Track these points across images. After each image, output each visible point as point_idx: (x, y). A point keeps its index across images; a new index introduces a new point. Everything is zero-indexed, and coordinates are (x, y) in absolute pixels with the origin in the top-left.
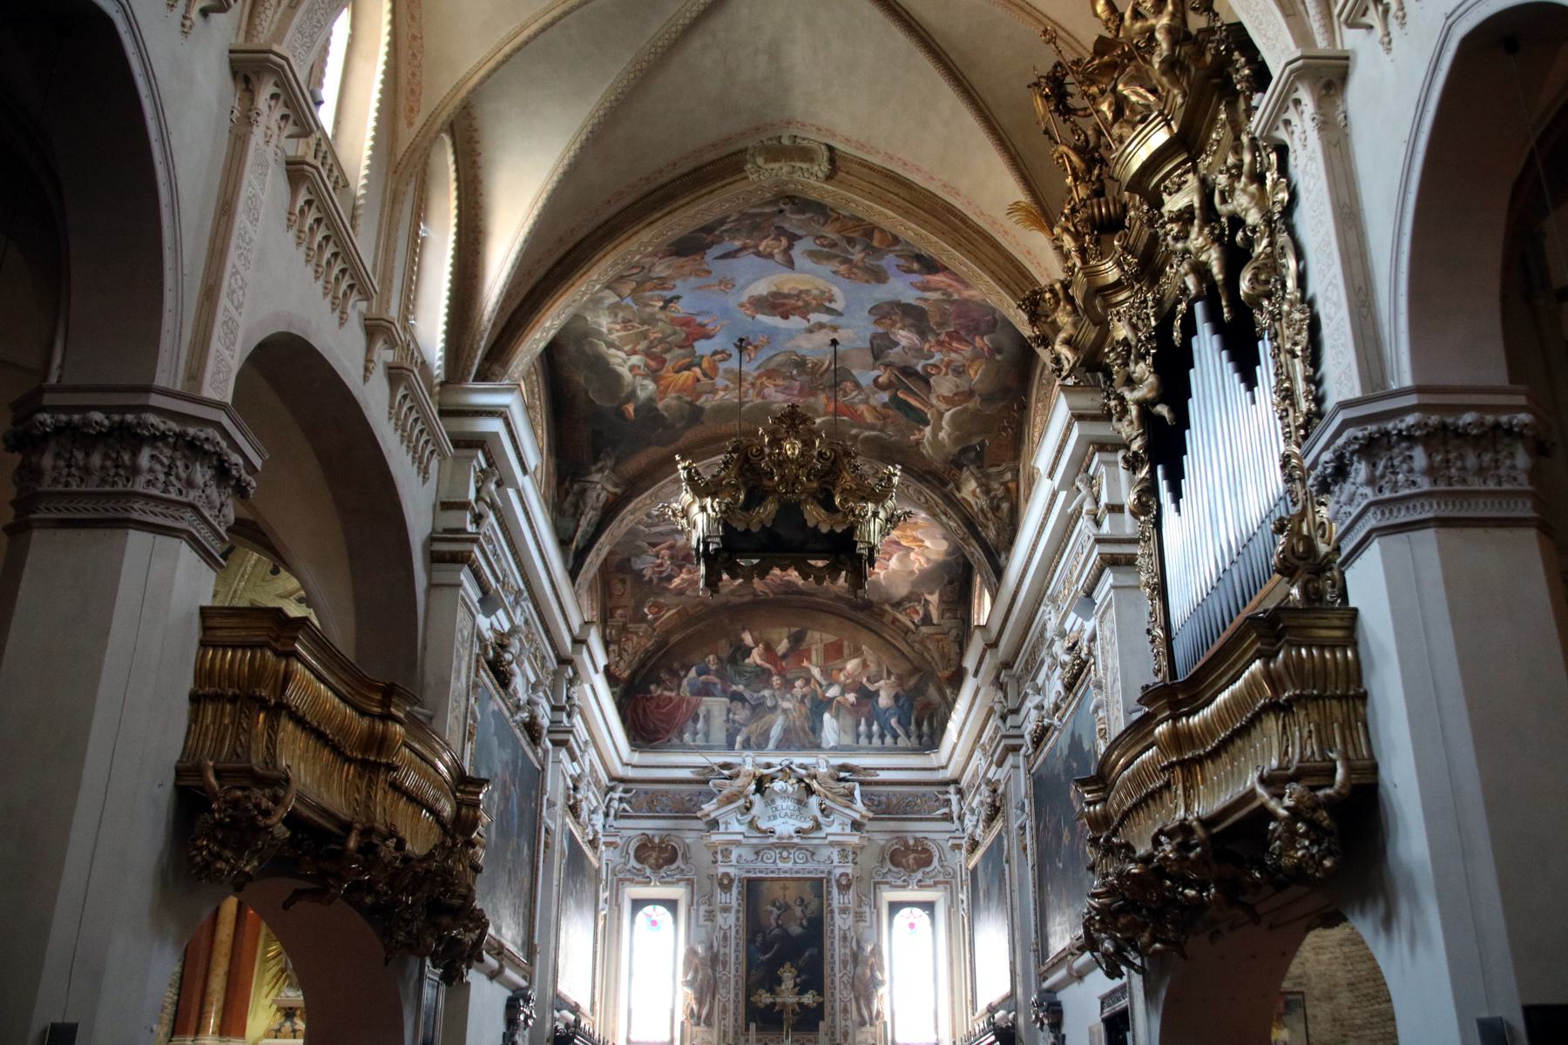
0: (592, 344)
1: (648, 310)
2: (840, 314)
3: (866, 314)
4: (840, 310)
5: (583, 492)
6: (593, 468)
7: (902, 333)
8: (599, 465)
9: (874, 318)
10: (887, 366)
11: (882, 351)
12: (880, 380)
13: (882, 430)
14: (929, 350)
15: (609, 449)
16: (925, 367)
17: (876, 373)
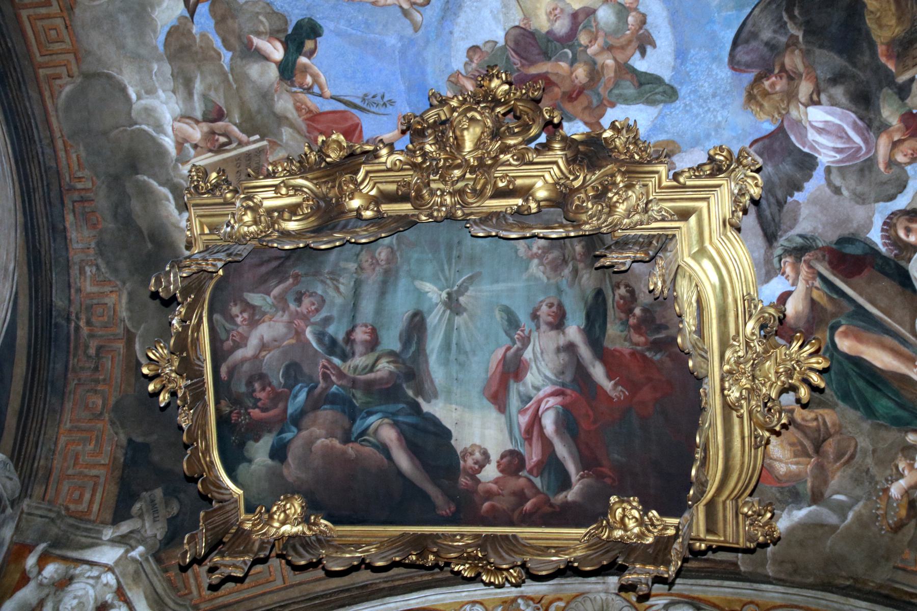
0: (144, 192)
1: (254, 70)
2: (670, 94)
3: (724, 73)
4: (666, 75)
5: (64, 583)
6: (108, 533)
7: (817, 115)
8: (125, 528)
9: (748, 77)
10: (798, 252)
11: (781, 204)
12: (793, 307)
13: (817, 498)
14: (891, 163)
15: (158, 493)
16: (889, 224)
17: (777, 286)
